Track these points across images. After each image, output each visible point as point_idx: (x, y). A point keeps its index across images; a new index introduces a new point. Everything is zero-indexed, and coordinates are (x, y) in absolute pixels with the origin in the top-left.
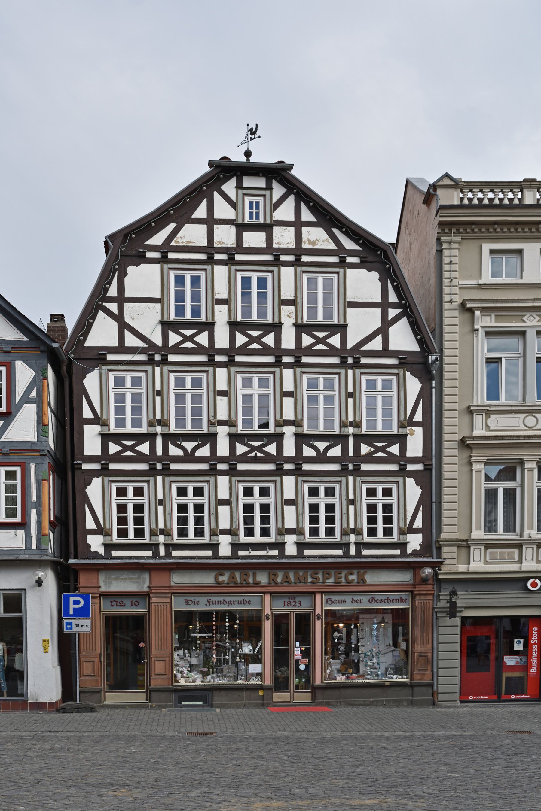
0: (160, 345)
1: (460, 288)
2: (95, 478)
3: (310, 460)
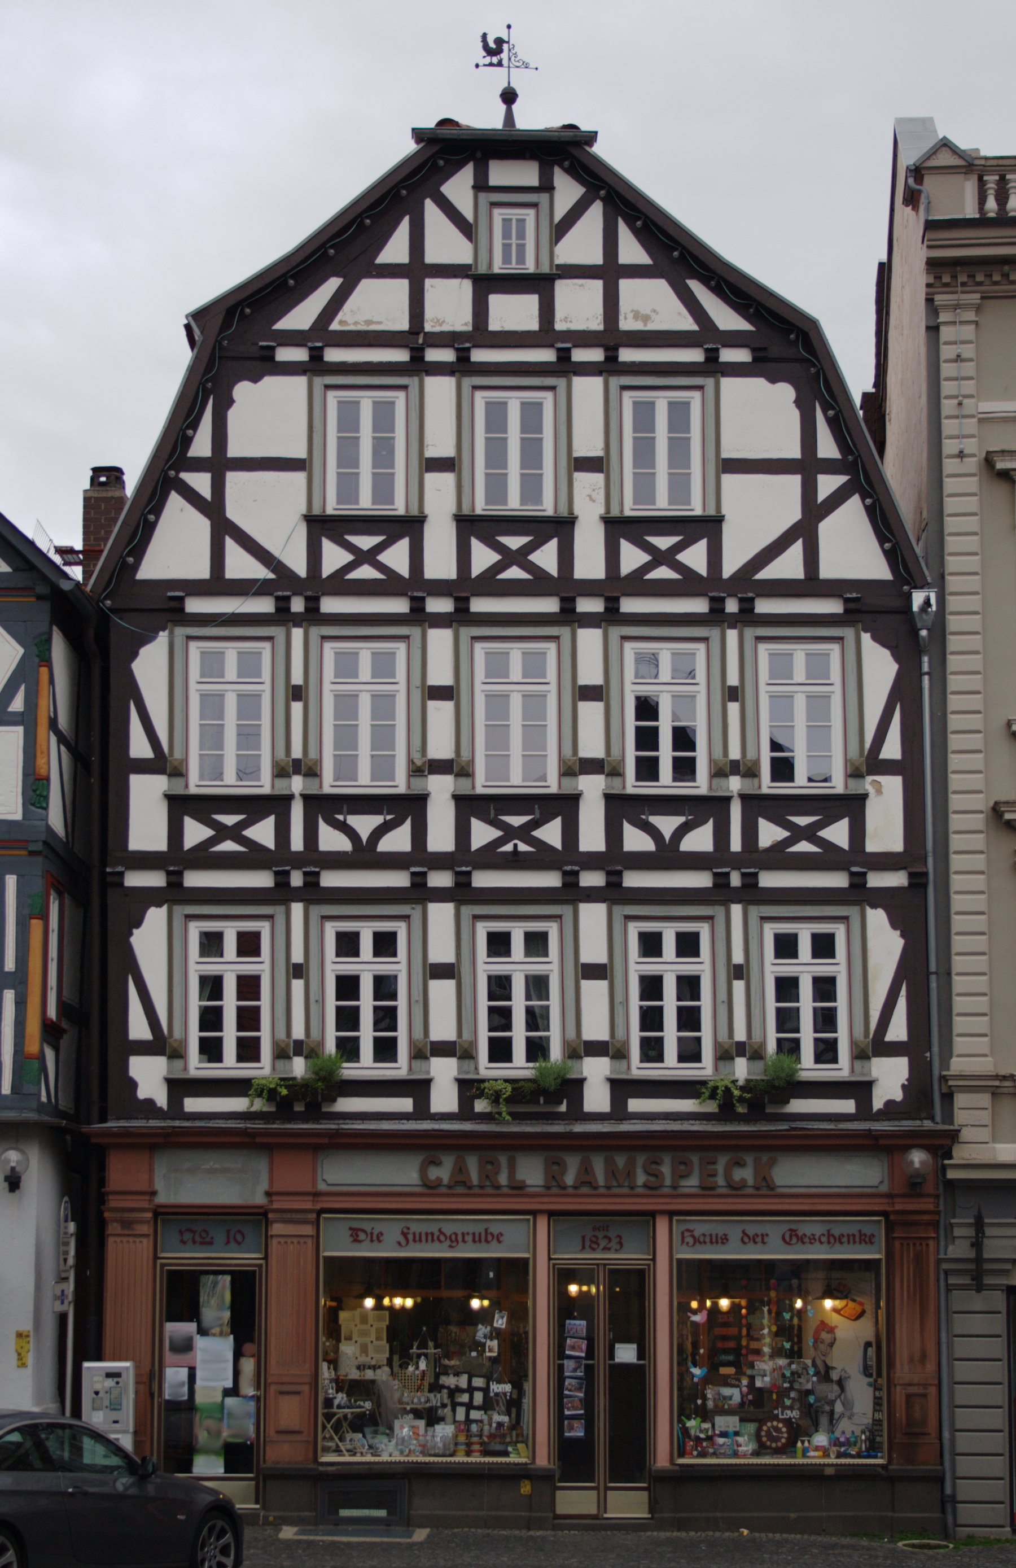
1: (980, 420)
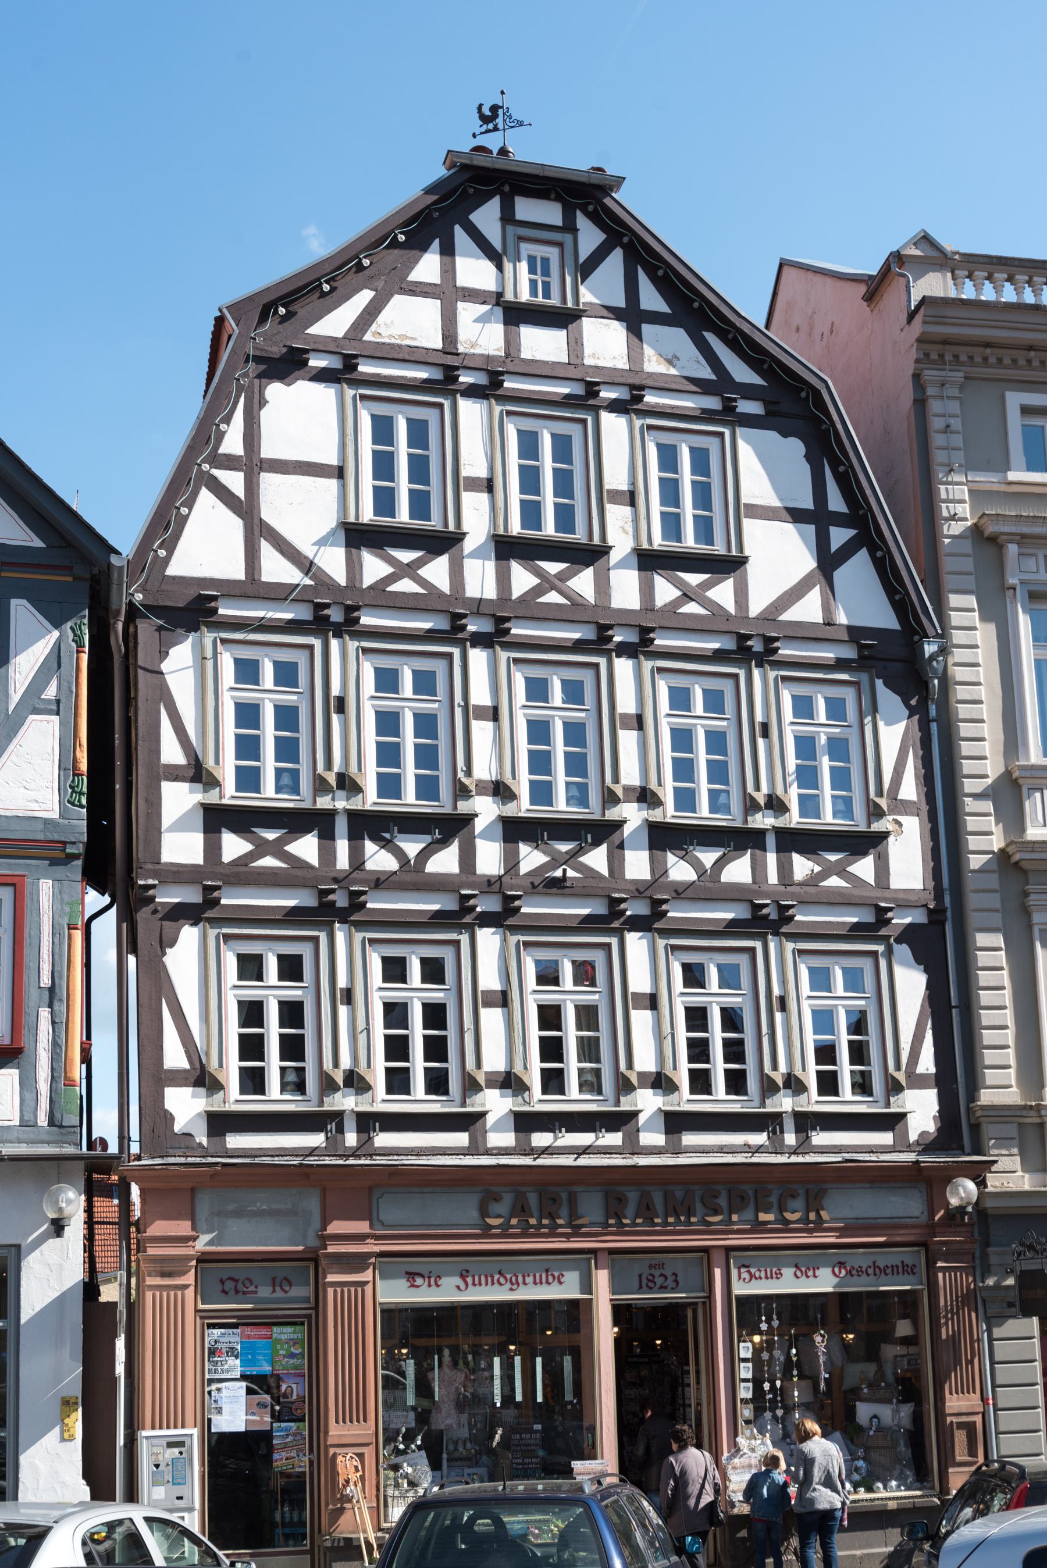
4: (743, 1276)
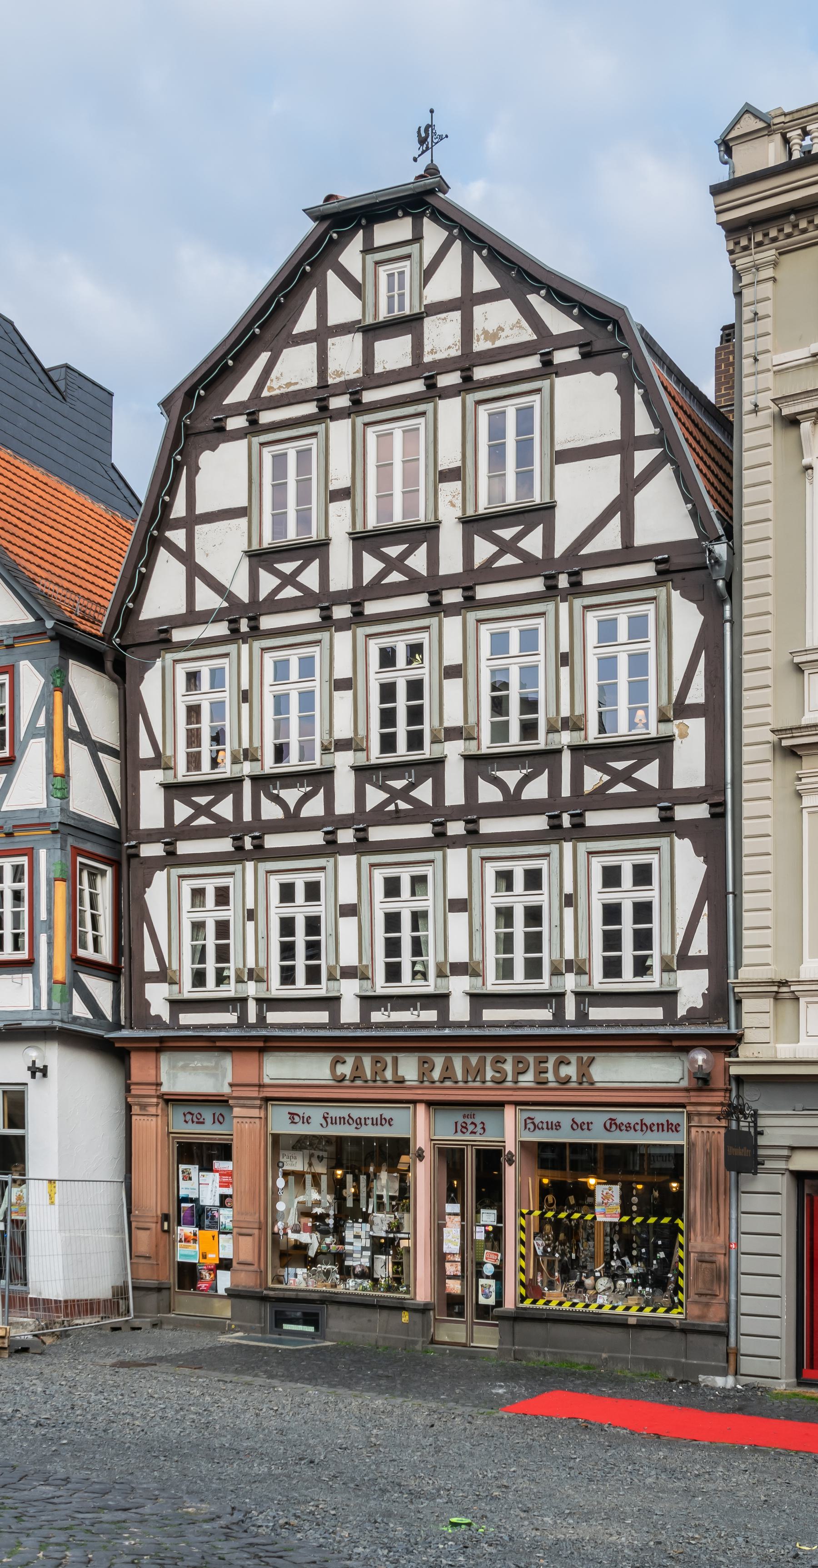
0: (246, 600)
2: (158, 872)
3: (494, 811)
4: (528, 1126)
